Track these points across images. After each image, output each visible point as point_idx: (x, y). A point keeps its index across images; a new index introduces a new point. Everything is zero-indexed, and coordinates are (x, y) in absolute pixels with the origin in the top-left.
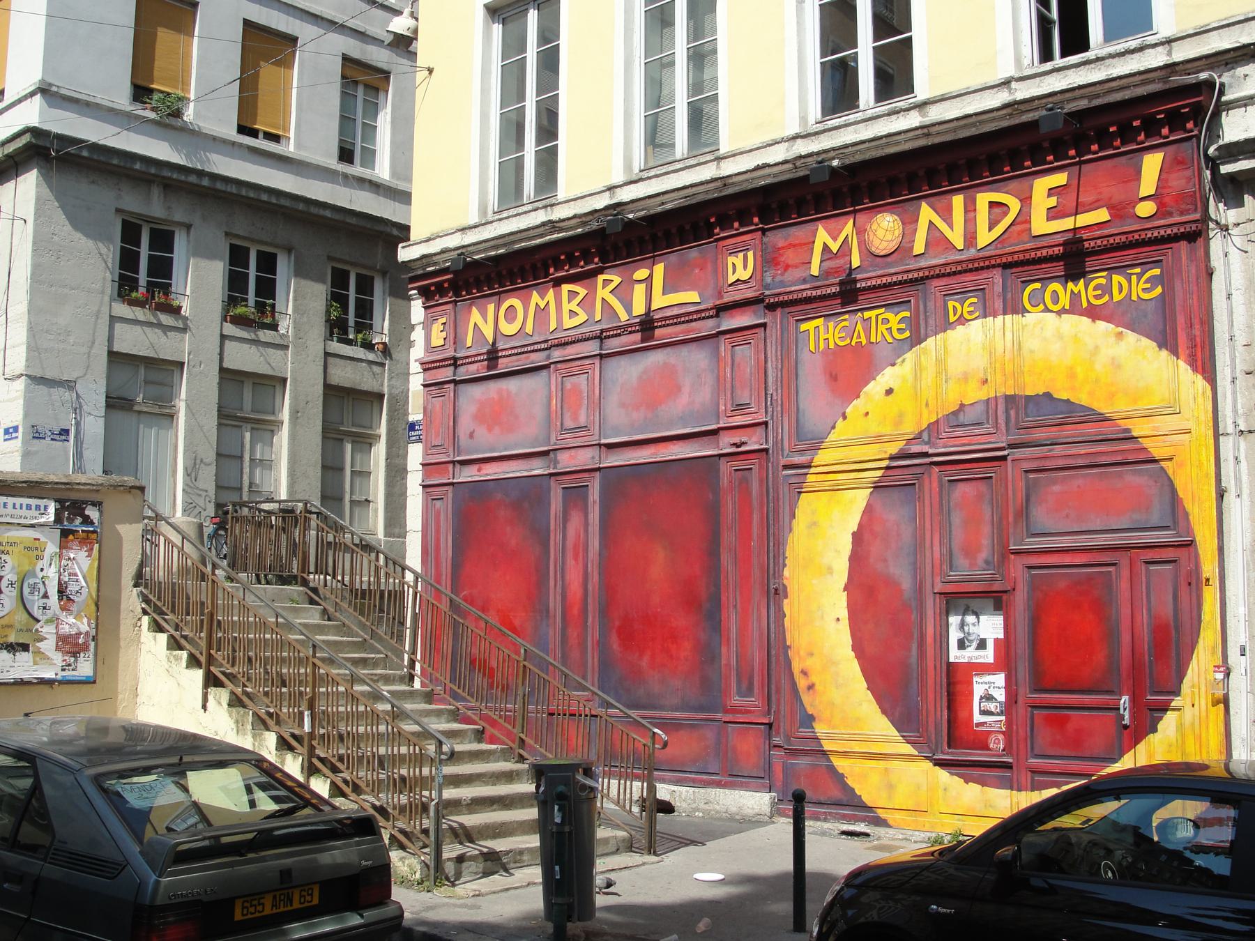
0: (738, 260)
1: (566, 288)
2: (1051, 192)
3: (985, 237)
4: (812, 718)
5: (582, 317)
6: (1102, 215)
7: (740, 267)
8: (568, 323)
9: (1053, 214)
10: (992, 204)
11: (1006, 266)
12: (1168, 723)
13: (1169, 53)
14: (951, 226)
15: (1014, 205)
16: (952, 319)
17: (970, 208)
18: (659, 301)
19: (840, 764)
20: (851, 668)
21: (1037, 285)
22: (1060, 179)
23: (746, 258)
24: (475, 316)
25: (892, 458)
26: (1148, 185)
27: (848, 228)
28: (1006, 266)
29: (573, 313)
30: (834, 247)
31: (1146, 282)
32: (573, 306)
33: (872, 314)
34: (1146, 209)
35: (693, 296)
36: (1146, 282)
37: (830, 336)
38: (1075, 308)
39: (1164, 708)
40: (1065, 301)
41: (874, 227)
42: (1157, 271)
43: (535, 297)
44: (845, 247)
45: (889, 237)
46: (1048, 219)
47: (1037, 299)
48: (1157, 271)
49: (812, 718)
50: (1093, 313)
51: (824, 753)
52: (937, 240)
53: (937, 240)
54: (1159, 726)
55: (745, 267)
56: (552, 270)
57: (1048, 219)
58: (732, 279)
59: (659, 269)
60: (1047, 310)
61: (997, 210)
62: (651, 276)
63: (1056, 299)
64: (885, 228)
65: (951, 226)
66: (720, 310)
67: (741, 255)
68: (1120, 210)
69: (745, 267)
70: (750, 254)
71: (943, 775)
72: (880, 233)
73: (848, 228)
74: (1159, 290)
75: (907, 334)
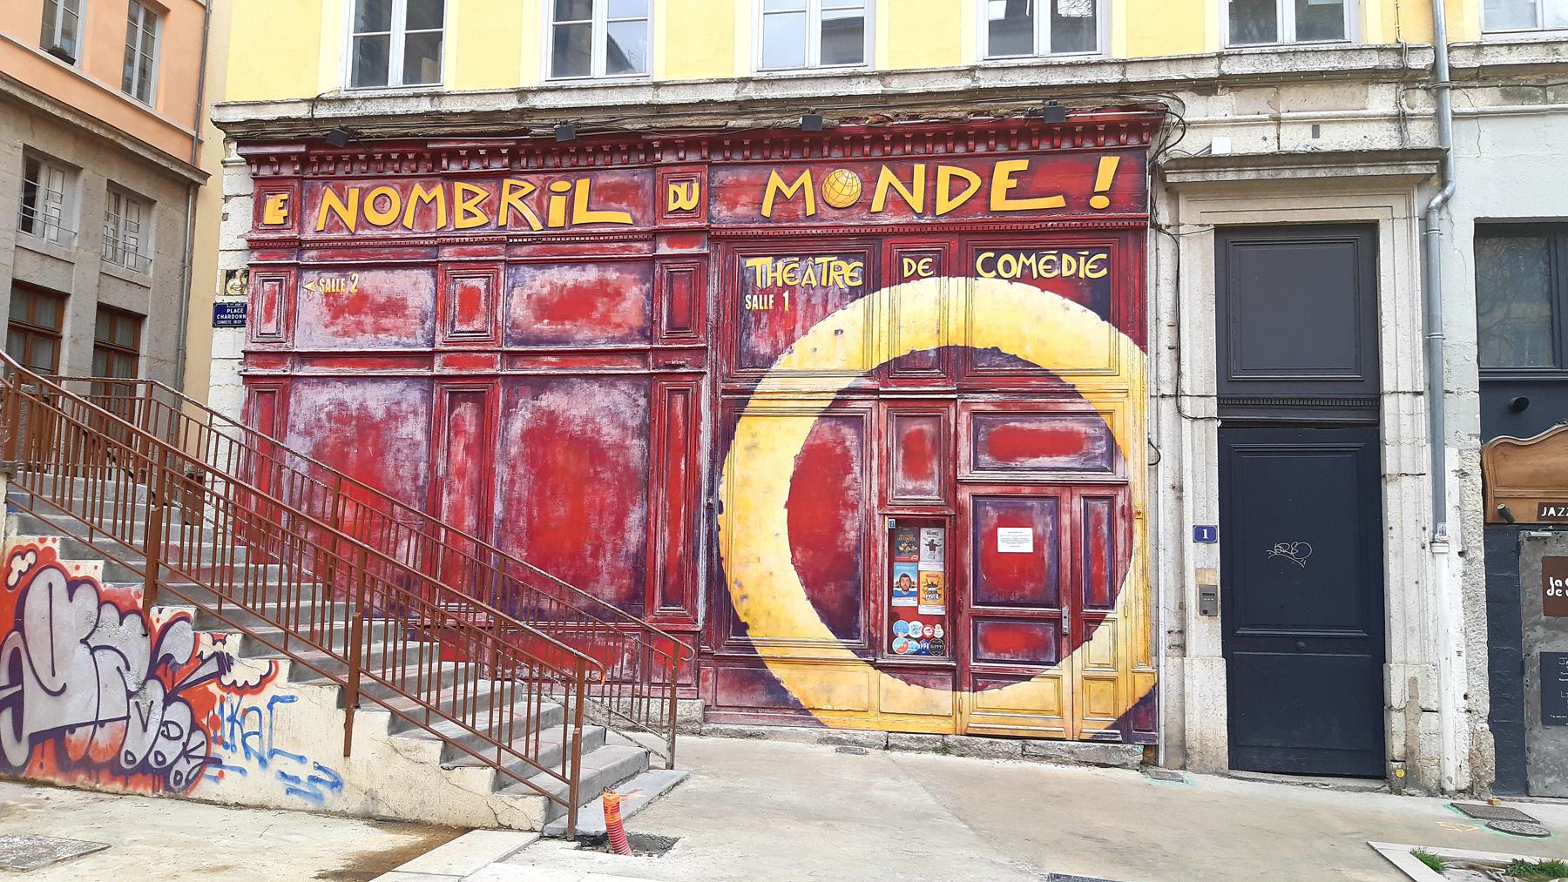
0: (682, 190)
1: (459, 187)
2: (1012, 175)
3: (944, 205)
4: (746, 626)
5: (481, 219)
6: (1058, 201)
7: (683, 197)
8: (460, 222)
9: (1011, 194)
10: (953, 177)
11: (961, 233)
12: (1102, 633)
13: (1124, 73)
14: (911, 191)
15: (976, 182)
16: (907, 274)
17: (932, 177)
18: (581, 215)
19: (777, 671)
20: (777, 520)
21: (992, 255)
22: (1022, 165)
23: (690, 189)
24: (330, 198)
25: (839, 392)
26: (1104, 181)
27: (806, 178)
28: (961, 233)
29: (469, 214)
30: (789, 193)
31: (1094, 263)
32: (470, 206)
33: (825, 260)
34: (1099, 202)
35: (626, 218)
36: (1094, 263)
37: (778, 275)
38: (1026, 277)
39: (1098, 620)
40: (1016, 270)
41: (832, 179)
42: (1104, 256)
43: (418, 190)
44: (800, 195)
45: (847, 191)
46: (1007, 198)
47: (989, 266)
48: (1104, 256)
49: (746, 626)
50: (1043, 284)
51: (760, 662)
52: (896, 202)
53: (896, 202)
54: (1094, 635)
55: (689, 199)
56: (445, 163)
57: (1007, 198)
58: (672, 206)
59: (583, 186)
60: (999, 276)
61: (958, 183)
62: (574, 188)
63: (1007, 266)
64: (844, 185)
65: (911, 191)
66: (654, 236)
67: (685, 185)
68: (1077, 201)
69: (689, 199)
70: (696, 186)
71: (886, 678)
72: (838, 186)
73: (806, 178)
74: (1105, 272)
75: (860, 282)
